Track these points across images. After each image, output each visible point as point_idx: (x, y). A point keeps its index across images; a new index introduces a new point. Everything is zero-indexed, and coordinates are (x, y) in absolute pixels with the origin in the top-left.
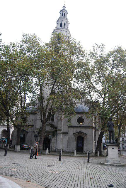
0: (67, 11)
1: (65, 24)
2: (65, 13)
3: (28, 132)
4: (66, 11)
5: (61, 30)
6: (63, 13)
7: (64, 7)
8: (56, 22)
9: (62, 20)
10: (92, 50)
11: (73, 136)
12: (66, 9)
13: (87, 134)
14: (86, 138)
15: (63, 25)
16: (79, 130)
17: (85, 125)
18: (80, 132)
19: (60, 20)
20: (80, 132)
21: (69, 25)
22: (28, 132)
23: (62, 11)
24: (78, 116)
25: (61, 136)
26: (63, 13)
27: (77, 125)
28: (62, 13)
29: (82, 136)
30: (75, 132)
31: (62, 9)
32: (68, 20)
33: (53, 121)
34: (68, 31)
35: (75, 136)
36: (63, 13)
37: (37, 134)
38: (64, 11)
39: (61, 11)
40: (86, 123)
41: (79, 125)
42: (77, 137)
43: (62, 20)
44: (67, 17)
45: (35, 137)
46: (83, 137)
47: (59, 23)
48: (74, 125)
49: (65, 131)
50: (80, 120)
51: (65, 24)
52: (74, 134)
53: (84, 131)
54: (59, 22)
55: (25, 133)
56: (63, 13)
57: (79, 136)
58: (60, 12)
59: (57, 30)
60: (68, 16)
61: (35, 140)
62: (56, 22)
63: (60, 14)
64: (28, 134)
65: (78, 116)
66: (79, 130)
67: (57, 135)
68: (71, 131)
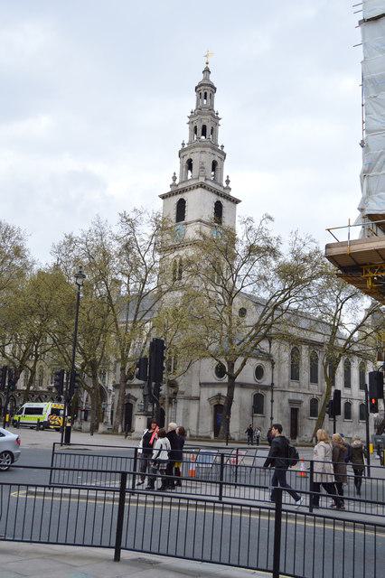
3: (136, 400)
5: (192, 151)
7: (207, 71)
15: (199, 131)
16: (216, 391)
20: (219, 395)
21: (220, 122)
22: (136, 400)
25: (181, 405)
27: (214, 381)
31: (200, 78)
36: (206, 91)
39: (196, 88)
42: (215, 406)
55: (132, 401)
56: (206, 91)
66: (216, 391)
67: (176, 402)
68: (207, 394)
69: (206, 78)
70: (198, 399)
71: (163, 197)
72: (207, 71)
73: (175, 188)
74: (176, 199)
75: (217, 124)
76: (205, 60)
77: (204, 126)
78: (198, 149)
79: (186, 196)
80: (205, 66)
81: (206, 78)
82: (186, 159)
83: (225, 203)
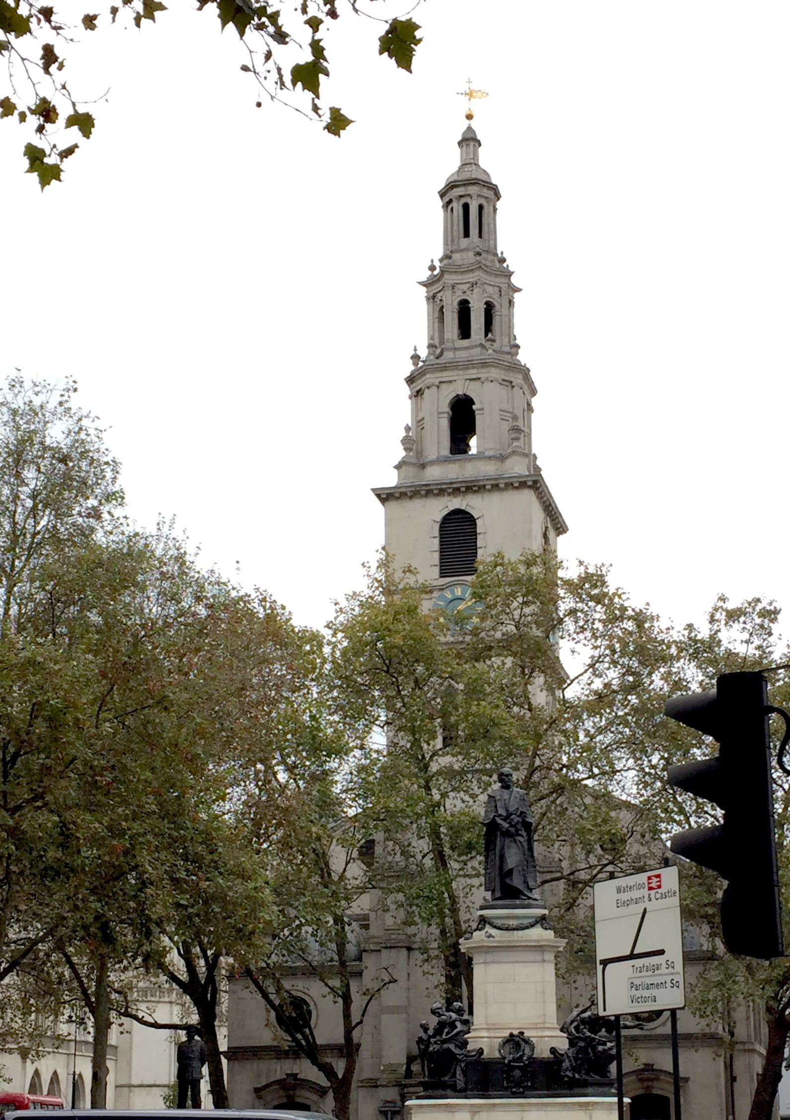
1: (489, 309)
2: (481, 208)
4: (486, 192)
5: (473, 373)
6: (466, 207)
7: (469, 140)
9: (471, 278)
10: (704, 632)
26: (466, 207)
28: (457, 207)
32: (509, 274)
34: (518, 379)
38: (473, 190)
39: (451, 186)
44: (503, 246)
51: (489, 309)
59: (446, 375)
60: (511, 233)
63: (447, 205)
69: (470, 162)
71: (385, 496)
72: (469, 140)
74: (437, 509)
75: (511, 303)
76: (464, 105)
77: (471, 307)
78: (494, 373)
79: (473, 504)
80: (466, 123)
81: (470, 162)
83: (551, 534)
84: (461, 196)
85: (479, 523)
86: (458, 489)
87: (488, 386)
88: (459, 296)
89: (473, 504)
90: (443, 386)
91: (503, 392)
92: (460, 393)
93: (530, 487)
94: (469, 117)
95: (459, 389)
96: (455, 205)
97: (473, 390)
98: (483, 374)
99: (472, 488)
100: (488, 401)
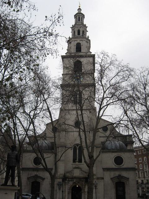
0: (84, 15)
1: (83, 32)
2: (82, 18)
3: (43, 179)
5: (81, 39)
6: (79, 17)
7: (79, 9)
8: (71, 28)
9: (80, 26)
11: (110, 182)
12: (82, 12)
13: (128, 178)
14: (127, 183)
15: (81, 33)
17: (125, 166)
18: (120, 177)
19: (78, 26)
20: (120, 176)
22: (43, 179)
23: (79, 15)
24: (115, 155)
26: (79, 17)
27: (114, 167)
28: (78, 17)
29: (123, 180)
30: (112, 177)
31: (77, 12)
33: (82, 162)
34: (89, 42)
35: (113, 182)
36: (79, 17)
37: (62, 181)
38: (80, 15)
39: (77, 14)
40: (125, 165)
41: (117, 167)
42: (116, 183)
43: (80, 26)
45: (58, 185)
46: (124, 183)
47: (76, 30)
48: (111, 167)
49: (99, 176)
50: (119, 161)
52: (111, 179)
53: (125, 174)
54: (76, 28)
56: (79, 17)
57: (118, 181)
58: (75, 16)
59: (76, 39)
61: (60, 189)
62: (71, 28)
64: (45, 181)
65: (115, 155)
66: (117, 173)
68: (108, 176)
70: (103, 178)
72: (79, 9)
73: (68, 54)
79: (81, 60)
82: (76, 42)
84: (78, 16)
85: (82, 63)
86: (78, 56)
87: (84, 41)
88: (78, 29)
89: (81, 60)
90: (75, 41)
91: (86, 43)
92: (78, 42)
93: (92, 57)
94: (80, 7)
95: (78, 41)
96: (77, 17)
97: (81, 42)
98: (83, 39)
99: (82, 56)
100: (83, 44)
